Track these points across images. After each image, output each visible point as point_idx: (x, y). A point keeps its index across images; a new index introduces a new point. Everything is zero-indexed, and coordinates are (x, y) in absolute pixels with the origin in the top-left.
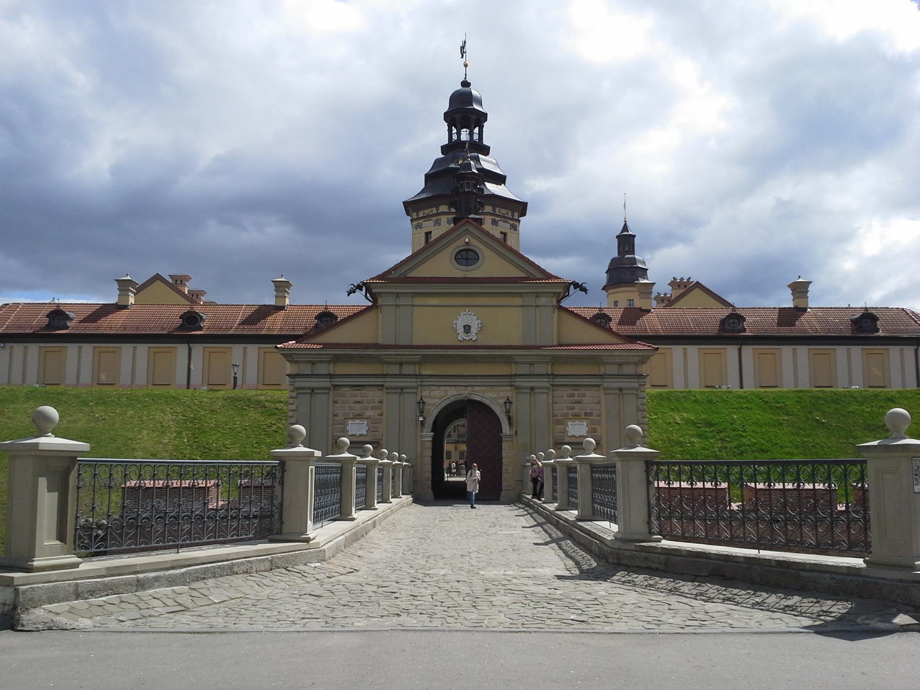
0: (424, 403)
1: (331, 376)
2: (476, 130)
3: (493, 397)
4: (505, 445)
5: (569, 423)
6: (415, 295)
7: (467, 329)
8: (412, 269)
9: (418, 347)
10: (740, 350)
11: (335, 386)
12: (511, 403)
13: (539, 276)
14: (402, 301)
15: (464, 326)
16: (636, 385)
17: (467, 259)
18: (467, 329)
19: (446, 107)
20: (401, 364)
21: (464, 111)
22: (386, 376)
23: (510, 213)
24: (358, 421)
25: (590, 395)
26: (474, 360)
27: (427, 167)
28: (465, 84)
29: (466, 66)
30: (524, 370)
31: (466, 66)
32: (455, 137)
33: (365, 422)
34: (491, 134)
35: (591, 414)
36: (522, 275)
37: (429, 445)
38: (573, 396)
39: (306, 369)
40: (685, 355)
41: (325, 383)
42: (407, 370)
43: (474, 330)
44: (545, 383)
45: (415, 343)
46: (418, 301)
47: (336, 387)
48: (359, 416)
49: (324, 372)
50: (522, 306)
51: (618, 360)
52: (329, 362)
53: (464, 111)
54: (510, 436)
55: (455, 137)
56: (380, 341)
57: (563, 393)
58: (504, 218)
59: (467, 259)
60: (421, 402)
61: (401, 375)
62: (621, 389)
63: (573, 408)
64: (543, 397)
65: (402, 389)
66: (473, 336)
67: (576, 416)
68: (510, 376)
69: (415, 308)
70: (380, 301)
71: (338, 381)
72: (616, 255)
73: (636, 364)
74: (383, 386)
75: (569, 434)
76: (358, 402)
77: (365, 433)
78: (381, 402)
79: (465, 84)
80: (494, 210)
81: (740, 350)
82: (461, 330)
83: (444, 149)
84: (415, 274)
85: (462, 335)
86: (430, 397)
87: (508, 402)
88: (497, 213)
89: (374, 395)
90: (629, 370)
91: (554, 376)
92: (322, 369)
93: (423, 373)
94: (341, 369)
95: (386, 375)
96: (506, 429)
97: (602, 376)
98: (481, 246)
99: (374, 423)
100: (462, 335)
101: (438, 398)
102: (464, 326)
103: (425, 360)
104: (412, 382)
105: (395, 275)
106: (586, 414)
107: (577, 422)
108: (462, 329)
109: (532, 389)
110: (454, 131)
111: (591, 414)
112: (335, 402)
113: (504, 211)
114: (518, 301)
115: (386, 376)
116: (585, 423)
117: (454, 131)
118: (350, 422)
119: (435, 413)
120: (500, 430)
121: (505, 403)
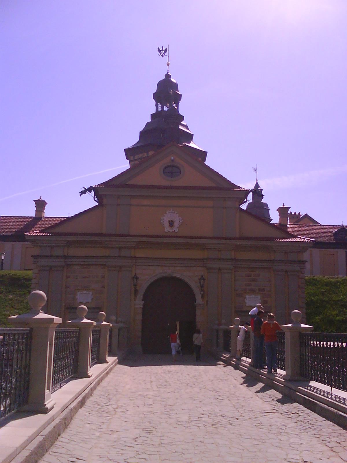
0: (137, 278)
1: (65, 257)
3: (190, 276)
5: (247, 296)
7: (171, 224)
9: (134, 236)
12: (204, 279)
15: (169, 221)
17: (172, 173)
18: (171, 224)
19: (155, 90)
20: (120, 249)
21: (167, 92)
24: (85, 292)
27: (142, 127)
28: (168, 76)
29: (168, 65)
31: (168, 65)
32: (160, 109)
33: (91, 293)
34: (183, 108)
36: (214, 185)
37: (141, 311)
43: (176, 224)
47: (68, 265)
48: (86, 288)
55: (160, 109)
56: (104, 232)
59: (172, 173)
60: (136, 277)
61: (120, 257)
65: (121, 267)
66: (175, 229)
67: (252, 291)
68: (203, 259)
70: (105, 201)
74: (105, 265)
75: (247, 305)
77: (90, 301)
78: (103, 277)
79: (168, 76)
82: (166, 224)
85: (167, 228)
87: (202, 278)
91: (237, 260)
92: (58, 252)
93: (138, 255)
94: (73, 251)
95: (108, 256)
96: (199, 300)
97: (273, 261)
100: (167, 228)
101: (148, 275)
102: (169, 221)
106: (260, 290)
107: (253, 296)
108: (168, 223)
110: (159, 105)
112: (68, 277)
116: (259, 297)
117: (159, 105)
118: (79, 293)
119: (146, 286)
120: (194, 300)
121: (200, 279)
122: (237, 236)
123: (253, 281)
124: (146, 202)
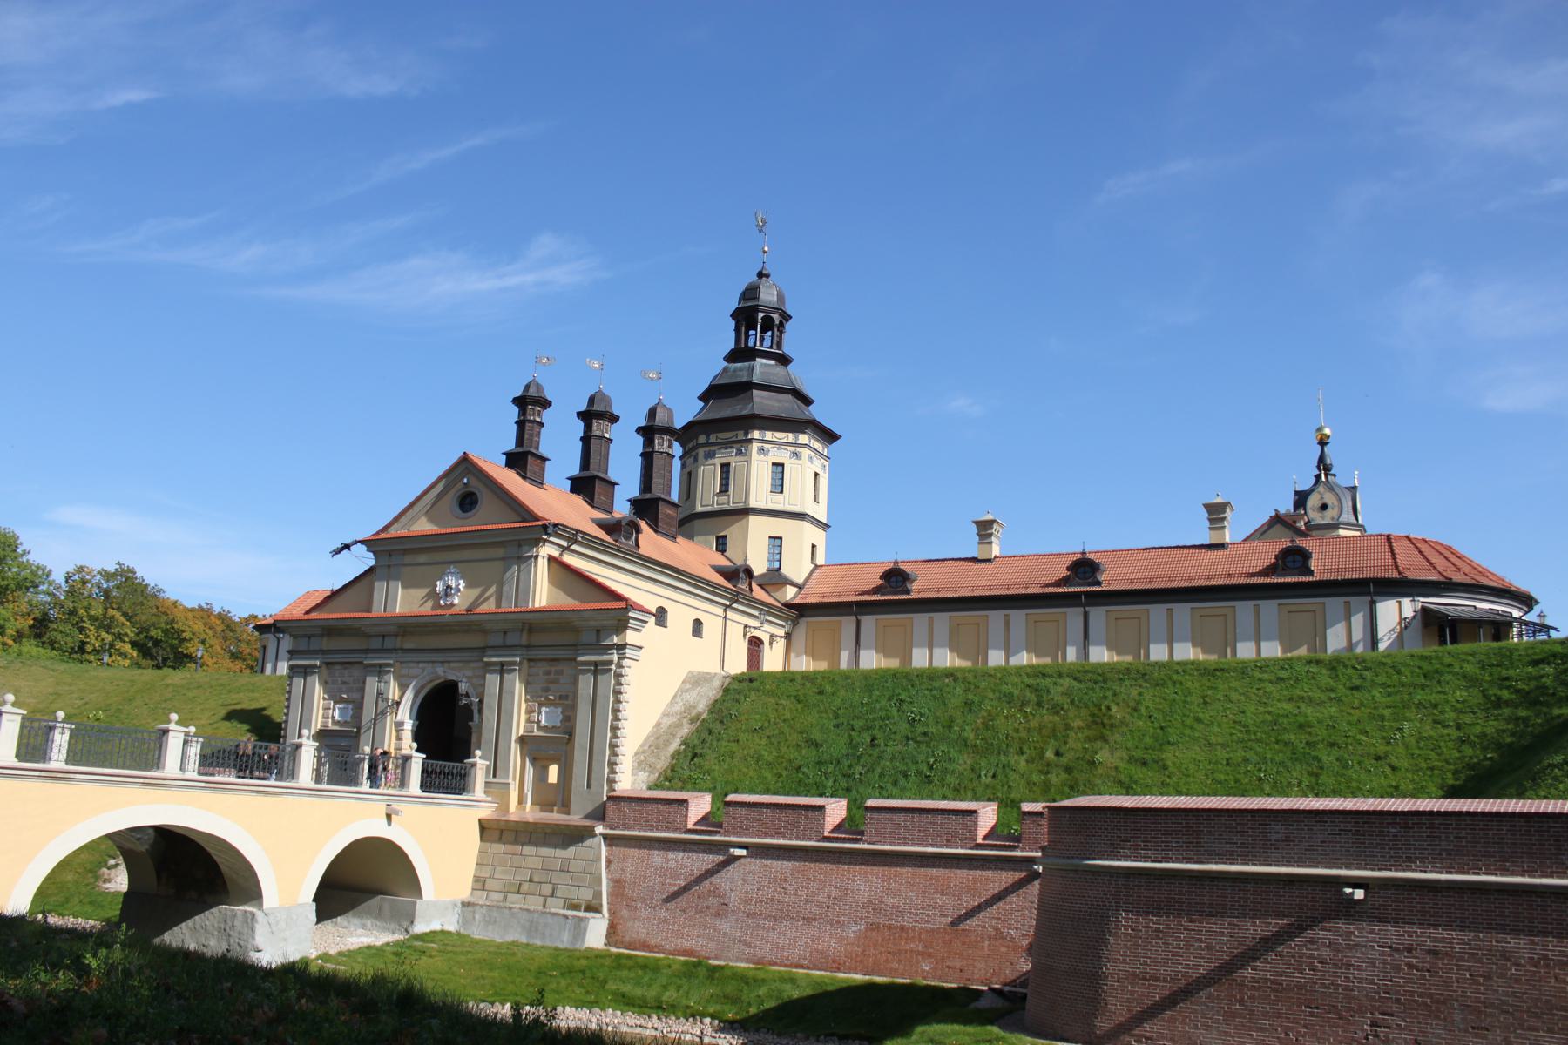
1: (323, 652)
11: (328, 664)
22: (366, 651)
35: (566, 697)
39: (303, 645)
42: (389, 643)
46: (408, 559)
50: (503, 559)
52: (322, 635)
58: (779, 444)
76: (344, 683)
83: (733, 357)
93: (407, 645)
98: (481, 486)
113: (780, 436)
114: (500, 552)
124: (422, 558)
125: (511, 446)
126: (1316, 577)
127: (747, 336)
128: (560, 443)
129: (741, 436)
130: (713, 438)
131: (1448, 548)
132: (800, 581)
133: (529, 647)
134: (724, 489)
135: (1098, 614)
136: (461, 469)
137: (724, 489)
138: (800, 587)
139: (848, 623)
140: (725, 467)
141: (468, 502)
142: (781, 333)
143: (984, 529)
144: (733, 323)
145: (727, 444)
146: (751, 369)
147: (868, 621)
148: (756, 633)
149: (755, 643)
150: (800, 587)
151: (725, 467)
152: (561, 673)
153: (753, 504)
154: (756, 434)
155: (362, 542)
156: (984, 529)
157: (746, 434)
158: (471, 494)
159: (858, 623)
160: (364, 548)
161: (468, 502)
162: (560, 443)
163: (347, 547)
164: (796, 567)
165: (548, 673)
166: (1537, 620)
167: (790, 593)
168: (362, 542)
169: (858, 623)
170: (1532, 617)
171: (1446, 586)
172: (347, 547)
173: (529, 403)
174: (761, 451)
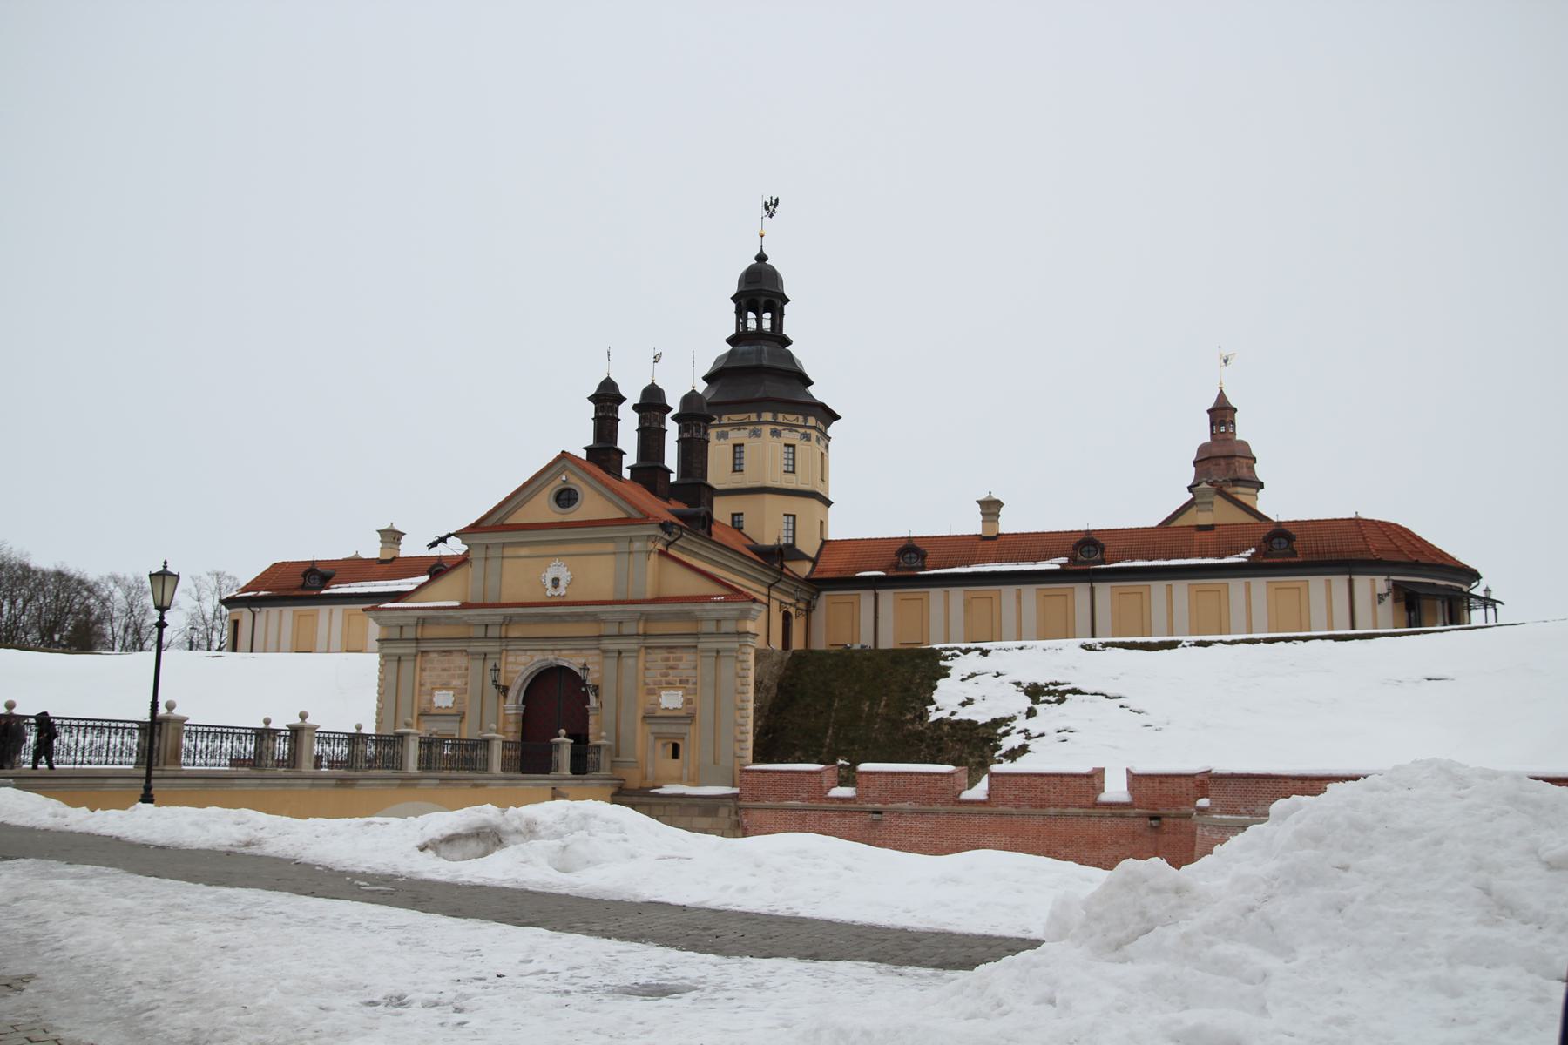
2: (767, 315)
4: (592, 720)
6: (504, 545)
8: (508, 515)
10: (1092, 590)
13: (638, 516)
14: (493, 553)
16: (736, 645)
19: (734, 290)
21: (760, 291)
23: (801, 418)
25: (688, 657)
26: (560, 618)
28: (761, 258)
30: (613, 629)
35: (687, 682)
38: (667, 659)
40: (1019, 598)
41: (409, 649)
43: (563, 583)
44: (632, 644)
45: (504, 600)
46: (508, 552)
49: (497, 634)
51: (714, 615)
53: (760, 291)
54: (596, 709)
57: (659, 656)
58: (791, 427)
62: (718, 651)
63: (666, 675)
64: (631, 662)
66: (562, 590)
67: (670, 685)
68: (600, 637)
69: (506, 562)
71: (425, 646)
72: (1208, 439)
73: (738, 619)
79: (761, 258)
80: (775, 417)
81: (1092, 590)
82: (549, 584)
84: (510, 521)
85: (550, 591)
86: (515, 663)
88: (780, 420)
89: (459, 661)
90: (728, 627)
93: (512, 634)
94: (431, 632)
97: (696, 635)
99: (460, 693)
103: (508, 621)
104: (493, 647)
105: (490, 523)
109: (620, 652)
111: (687, 682)
112: (422, 670)
114: (610, 547)
115: (470, 638)
122: (649, 596)
123: (671, 668)
124: (524, 551)
125: (590, 441)
126: (1300, 559)
127: (746, 319)
128: (628, 438)
129: (754, 417)
130: (725, 420)
131: (1406, 530)
132: (813, 555)
133: (645, 635)
134: (737, 468)
135: (1104, 590)
136: (559, 466)
137: (737, 468)
138: (814, 562)
139: (866, 597)
140: (738, 447)
141: (566, 498)
142: (782, 315)
143: (991, 508)
144: (733, 306)
145: (739, 426)
146: (760, 352)
147: (887, 596)
148: (792, 610)
149: (787, 617)
150: (814, 562)
151: (738, 447)
152: (680, 659)
153: (769, 484)
154: (767, 416)
155: (456, 534)
156: (991, 508)
157: (759, 416)
158: (569, 490)
159: (876, 596)
160: (458, 540)
161: (566, 498)
162: (628, 438)
163: (443, 540)
164: (808, 546)
165: (667, 659)
166: (1482, 594)
167: (804, 569)
168: (456, 534)
169: (876, 596)
170: (1478, 591)
171: (1414, 566)
172: (443, 540)
173: (607, 398)
174: (775, 433)
